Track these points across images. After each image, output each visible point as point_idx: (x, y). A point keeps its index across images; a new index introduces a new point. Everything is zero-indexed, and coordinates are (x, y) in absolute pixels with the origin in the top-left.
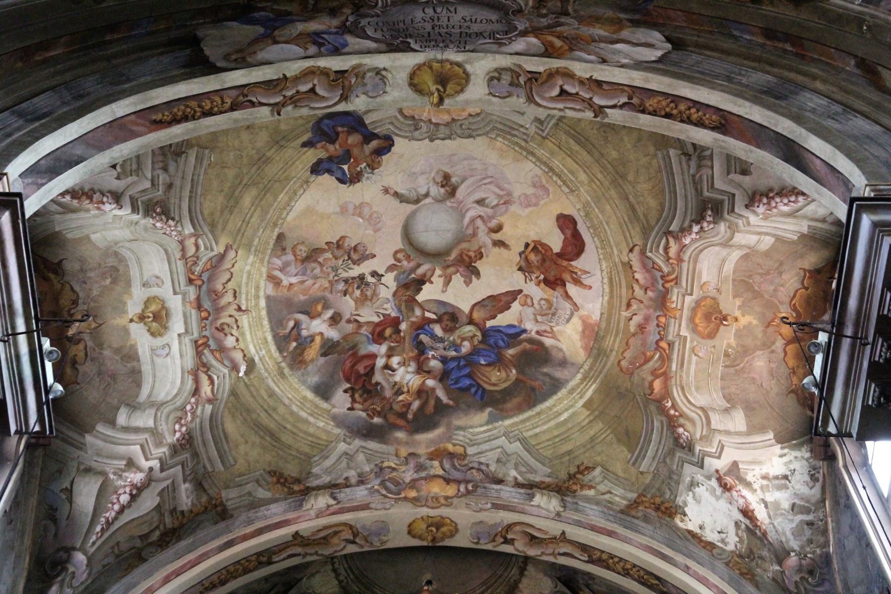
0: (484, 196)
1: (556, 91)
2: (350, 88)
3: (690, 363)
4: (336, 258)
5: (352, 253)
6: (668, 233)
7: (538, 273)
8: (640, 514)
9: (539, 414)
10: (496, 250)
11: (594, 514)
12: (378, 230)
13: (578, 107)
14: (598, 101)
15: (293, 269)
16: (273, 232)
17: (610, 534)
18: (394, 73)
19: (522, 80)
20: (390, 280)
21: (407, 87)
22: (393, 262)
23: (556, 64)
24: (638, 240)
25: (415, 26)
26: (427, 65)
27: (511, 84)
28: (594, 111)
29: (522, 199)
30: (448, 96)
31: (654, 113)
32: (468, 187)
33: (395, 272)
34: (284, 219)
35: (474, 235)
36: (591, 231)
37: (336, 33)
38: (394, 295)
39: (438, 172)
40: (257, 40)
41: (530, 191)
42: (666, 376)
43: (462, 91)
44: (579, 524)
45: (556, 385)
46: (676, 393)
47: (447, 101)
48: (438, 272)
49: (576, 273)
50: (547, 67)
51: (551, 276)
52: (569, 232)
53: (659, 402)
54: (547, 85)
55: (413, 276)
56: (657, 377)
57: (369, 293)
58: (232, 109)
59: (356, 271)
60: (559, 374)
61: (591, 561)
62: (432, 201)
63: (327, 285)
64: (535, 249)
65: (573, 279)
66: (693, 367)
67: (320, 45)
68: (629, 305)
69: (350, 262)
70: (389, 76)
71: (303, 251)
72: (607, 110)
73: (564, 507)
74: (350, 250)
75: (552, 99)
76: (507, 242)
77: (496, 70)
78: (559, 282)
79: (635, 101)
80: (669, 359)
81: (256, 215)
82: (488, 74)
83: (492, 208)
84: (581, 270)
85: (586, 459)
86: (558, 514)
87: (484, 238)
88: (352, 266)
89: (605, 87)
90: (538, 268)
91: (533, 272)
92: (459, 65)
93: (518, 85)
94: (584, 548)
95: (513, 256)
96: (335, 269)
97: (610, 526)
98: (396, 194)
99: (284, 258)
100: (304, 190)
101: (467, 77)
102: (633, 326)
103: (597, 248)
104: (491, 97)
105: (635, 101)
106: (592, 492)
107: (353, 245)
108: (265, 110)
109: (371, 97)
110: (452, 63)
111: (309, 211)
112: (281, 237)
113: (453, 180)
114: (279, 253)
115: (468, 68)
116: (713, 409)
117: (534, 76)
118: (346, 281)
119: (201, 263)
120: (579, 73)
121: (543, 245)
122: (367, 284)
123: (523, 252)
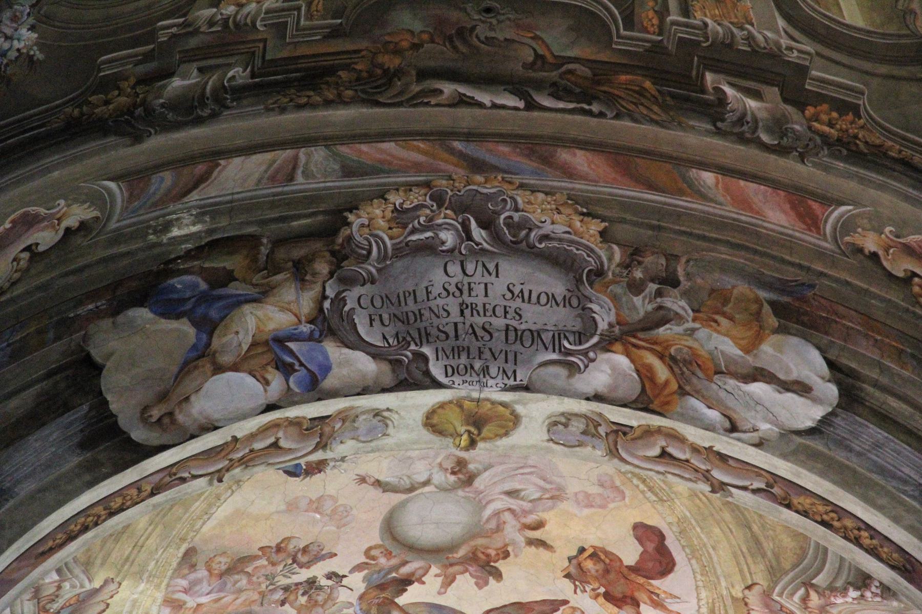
0: (518, 487)
1: (656, 451)
2: (331, 436)
4: (273, 564)
5: (299, 555)
6: (808, 585)
7: (596, 585)
10: (533, 549)
12: (344, 525)
13: (687, 476)
14: (719, 475)
15: (205, 587)
16: (179, 548)
18: (402, 413)
19: (602, 430)
20: (357, 582)
21: (421, 427)
22: (363, 559)
23: (656, 421)
24: (761, 578)
25: (432, 304)
26: (459, 404)
27: (584, 433)
28: (712, 485)
29: (581, 497)
30: (484, 439)
31: (805, 514)
32: (494, 476)
33: (366, 571)
34: (198, 531)
35: (499, 529)
36: (688, 551)
37: (310, 338)
38: (361, 598)
39: (448, 457)
40: (187, 367)
41: (595, 490)
43: (506, 434)
47: (481, 445)
48: (434, 570)
49: (658, 595)
50: (643, 422)
51: (619, 590)
52: (651, 547)
54: (640, 442)
55: (394, 575)
57: (320, 598)
58: (152, 494)
59: (303, 575)
62: (435, 490)
63: (256, 596)
64: (594, 556)
65: (652, 601)
67: (287, 370)
69: (295, 565)
70: (395, 417)
71: (222, 563)
72: (733, 490)
74: (296, 553)
75: (648, 459)
76: (548, 542)
77: (563, 414)
78: (629, 600)
79: (776, 490)
81: (154, 535)
82: (549, 418)
83: (531, 501)
84: (665, 592)
87: (512, 532)
88: (298, 570)
89: (731, 462)
90: (597, 578)
91: (589, 583)
92: (504, 405)
93: (597, 435)
95: (560, 559)
96: (270, 578)
98: (378, 483)
99: (192, 576)
100: (233, 492)
101: (516, 419)
103: (694, 572)
104: (551, 444)
105: (776, 490)
107: (301, 546)
108: (202, 482)
109: (364, 442)
110: (493, 403)
111: (238, 514)
112: (190, 553)
113: (471, 467)
114: (186, 571)
115: (519, 409)
117: (621, 430)
118: (286, 589)
119: (60, 602)
120: (691, 439)
121: (606, 553)
122: (320, 588)
123: (575, 557)
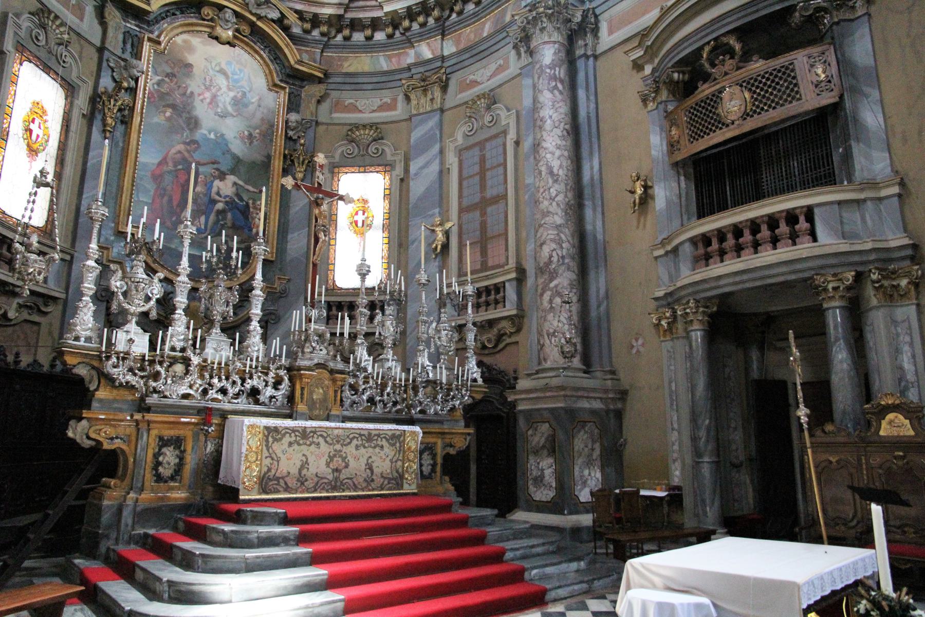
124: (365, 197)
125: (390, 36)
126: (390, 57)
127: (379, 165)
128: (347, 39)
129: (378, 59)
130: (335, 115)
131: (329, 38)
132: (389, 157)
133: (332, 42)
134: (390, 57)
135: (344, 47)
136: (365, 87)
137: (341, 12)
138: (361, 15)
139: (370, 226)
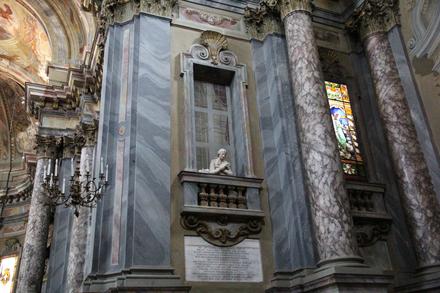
3: (41, 44)
8: (29, 70)
9: (4, 42)
11: (17, 68)
17: (20, 74)
42: (35, 46)
44: (13, 70)
45: (8, 38)
46: (37, 50)
53: (33, 51)
56: (33, 45)
60: (8, 36)
61: (15, 79)
66: (42, 46)
68: (25, 28)
73: (10, 65)
80: (36, 42)
85: (17, 54)
86: (8, 67)
94: (13, 76)
97: (21, 72)
102: (27, 33)
106: (19, 61)
116: (46, 56)
124: (8, 268)
125: (24, 199)
126: (25, 207)
127: (15, 254)
128: (11, 202)
129: (22, 209)
130: (5, 234)
131: (4, 204)
132: (18, 250)
133: (6, 204)
134: (25, 207)
135: (10, 205)
136: (16, 221)
137: (5, 194)
138: (13, 194)
139: (8, 280)
